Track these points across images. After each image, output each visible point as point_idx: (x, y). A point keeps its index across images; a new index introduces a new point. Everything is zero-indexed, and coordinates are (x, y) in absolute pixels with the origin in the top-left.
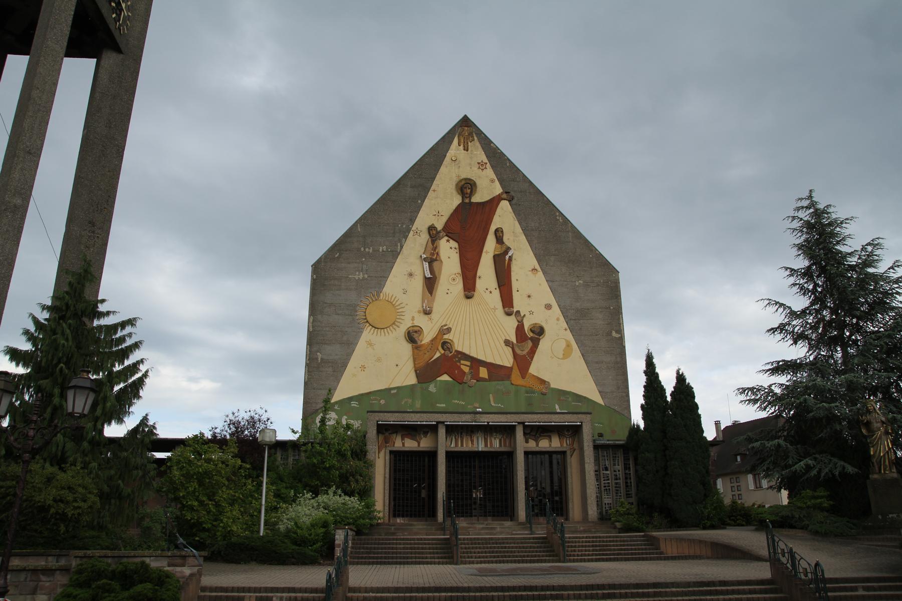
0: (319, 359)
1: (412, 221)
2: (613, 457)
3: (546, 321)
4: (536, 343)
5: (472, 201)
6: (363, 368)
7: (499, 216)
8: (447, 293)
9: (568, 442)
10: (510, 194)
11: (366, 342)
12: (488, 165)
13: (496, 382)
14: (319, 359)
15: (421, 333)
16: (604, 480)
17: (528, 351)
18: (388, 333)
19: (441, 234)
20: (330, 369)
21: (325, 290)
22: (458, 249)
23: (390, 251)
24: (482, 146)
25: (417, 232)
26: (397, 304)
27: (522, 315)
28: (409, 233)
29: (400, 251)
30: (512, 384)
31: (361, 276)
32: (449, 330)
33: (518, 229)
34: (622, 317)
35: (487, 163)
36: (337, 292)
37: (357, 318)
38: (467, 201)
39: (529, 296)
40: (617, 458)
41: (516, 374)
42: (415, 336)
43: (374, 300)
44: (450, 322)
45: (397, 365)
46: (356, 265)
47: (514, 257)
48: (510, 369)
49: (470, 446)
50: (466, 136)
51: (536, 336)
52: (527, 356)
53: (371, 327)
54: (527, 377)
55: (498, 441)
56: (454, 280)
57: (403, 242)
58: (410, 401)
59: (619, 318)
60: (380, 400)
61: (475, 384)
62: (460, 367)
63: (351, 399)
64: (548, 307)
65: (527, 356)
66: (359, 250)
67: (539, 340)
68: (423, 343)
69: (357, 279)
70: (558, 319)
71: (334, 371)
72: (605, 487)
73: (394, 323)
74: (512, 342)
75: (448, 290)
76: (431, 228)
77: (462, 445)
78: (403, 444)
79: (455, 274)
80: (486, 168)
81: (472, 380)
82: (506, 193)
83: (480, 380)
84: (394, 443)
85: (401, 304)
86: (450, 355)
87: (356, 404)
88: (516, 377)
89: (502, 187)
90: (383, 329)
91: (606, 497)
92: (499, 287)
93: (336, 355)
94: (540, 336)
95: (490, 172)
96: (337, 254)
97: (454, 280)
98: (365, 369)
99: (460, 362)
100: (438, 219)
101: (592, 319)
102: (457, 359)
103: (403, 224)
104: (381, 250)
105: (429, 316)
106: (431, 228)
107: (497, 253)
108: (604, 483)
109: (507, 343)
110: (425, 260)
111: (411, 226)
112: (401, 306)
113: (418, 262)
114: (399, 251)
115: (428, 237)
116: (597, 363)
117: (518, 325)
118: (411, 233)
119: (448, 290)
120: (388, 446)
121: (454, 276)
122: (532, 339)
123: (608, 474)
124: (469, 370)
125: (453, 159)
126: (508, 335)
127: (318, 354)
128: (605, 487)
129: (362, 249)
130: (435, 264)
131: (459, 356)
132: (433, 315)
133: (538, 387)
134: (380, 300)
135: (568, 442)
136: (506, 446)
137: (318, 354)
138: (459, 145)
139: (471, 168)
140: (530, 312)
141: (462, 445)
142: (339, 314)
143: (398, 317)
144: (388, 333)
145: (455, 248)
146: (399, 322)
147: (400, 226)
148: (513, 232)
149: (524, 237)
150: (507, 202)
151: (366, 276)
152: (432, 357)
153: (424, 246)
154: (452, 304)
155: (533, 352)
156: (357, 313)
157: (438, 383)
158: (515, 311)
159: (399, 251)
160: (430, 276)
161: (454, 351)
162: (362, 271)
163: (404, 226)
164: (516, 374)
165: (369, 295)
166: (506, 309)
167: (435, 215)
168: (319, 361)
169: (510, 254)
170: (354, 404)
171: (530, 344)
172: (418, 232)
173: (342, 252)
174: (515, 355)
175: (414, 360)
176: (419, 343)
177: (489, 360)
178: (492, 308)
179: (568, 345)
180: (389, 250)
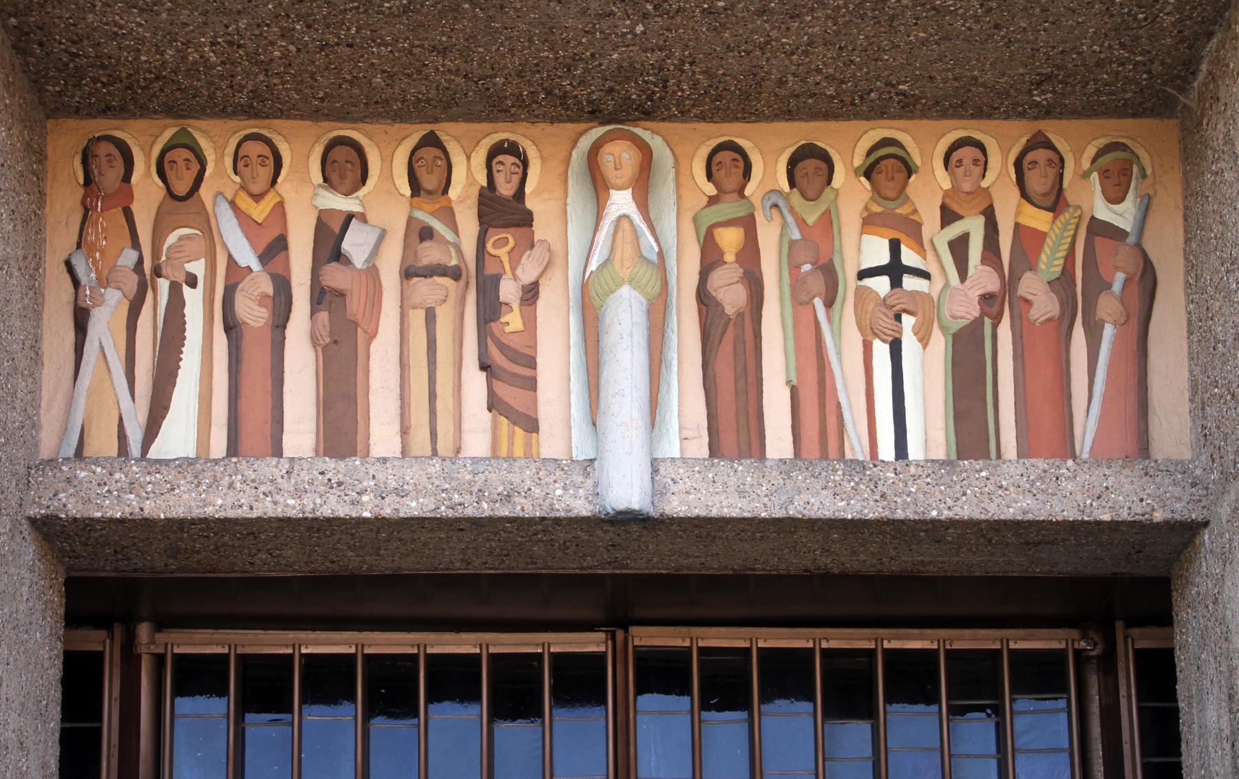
49: (477, 443)
136: (1066, 447)
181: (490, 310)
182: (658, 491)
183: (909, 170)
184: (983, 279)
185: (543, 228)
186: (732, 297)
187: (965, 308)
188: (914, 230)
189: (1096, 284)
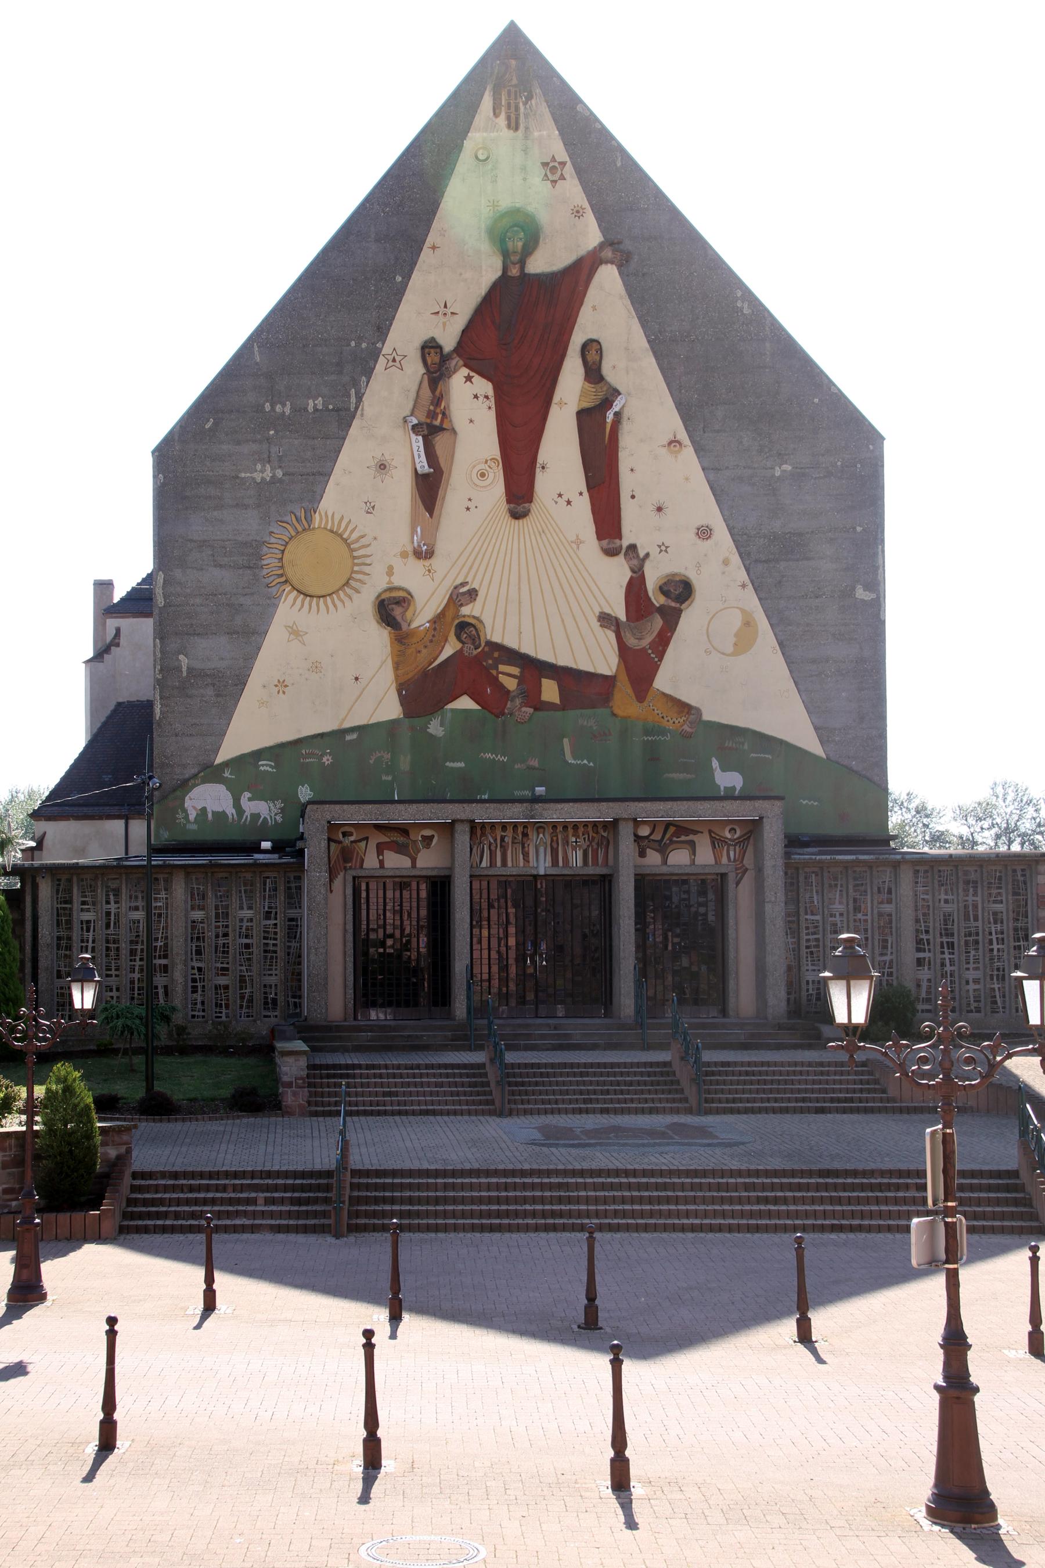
0: (184, 669)
1: (382, 331)
2: (830, 886)
3: (698, 566)
4: (671, 618)
5: (526, 271)
6: (282, 685)
7: (594, 308)
8: (468, 509)
9: (732, 854)
10: (621, 247)
11: (286, 626)
12: (569, 169)
13: (578, 712)
14: (184, 669)
15: (409, 605)
16: (808, 934)
17: (653, 641)
18: (335, 606)
19: (453, 363)
20: (210, 692)
21: (187, 508)
22: (493, 400)
23: (332, 410)
24: (553, 114)
25: (394, 360)
26: (354, 536)
27: (642, 554)
28: (376, 361)
29: (357, 408)
30: (614, 715)
31: (268, 474)
32: (473, 594)
33: (639, 340)
34: (883, 551)
35: (563, 164)
36: (215, 513)
37: (265, 572)
38: (514, 272)
39: (659, 509)
40: (839, 888)
41: (624, 690)
42: (397, 612)
43: (300, 529)
44: (475, 576)
45: (357, 679)
46: (255, 447)
47: (625, 415)
48: (609, 681)
49: (522, 864)
50: (515, 86)
51: (673, 604)
52: (650, 651)
53: (295, 592)
54: (649, 697)
55: (580, 853)
56: (483, 475)
57: (363, 384)
58: (387, 756)
59: (875, 554)
60: (322, 756)
61: (532, 715)
62: (497, 678)
63: (257, 755)
64: (704, 533)
65: (650, 651)
66: (259, 409)
67: (678, 613)
68: (414, 625)
69: (259, 480)
70: (726, 562)
71: (218, 696)
72: (807, 947)
73: (347, 584)
74: (617, 619)
75: (470, 500)
76: (429, 347)
77: (504, 863)
78: (381, 862)
79: (486, 462)
80: (562, 178)
81: (524, 709)
82: (612, 244)
83: (540, 706)
84: (362, 861)
85: (362, 537)
86: (475, 652)
87: (271, 766)
88: (624, 702)
89: (602, 232)
90: (323, 596)
91: (810, 968)
92: (589, 488)
93: (222, 659)
94: (682, 603)
95: (573, 190)
96: (208, 421)
97: (483, 475)
98: (286, 690)
99: (497, 669)
100: (444, 324)
101: (808, 559)
102: (490, 662)
103: (360, 339)
104: (310, 409)
105: (427, 563)
106: (429, 347)
107: (586, 405)
108: (808, 940)
109: (606, 620)
110: (415, 429)
111: (379, 345)
112: (363, 541)
113: (399, 434)
114: (353, 406)
115: (422, 370)
116: (814, 661)
117: (631, 578)
118: (382, 362)
119: (470, 500)
120: (351, 868)
121: (483, 466)
122: (662, 610)
123: (818, 921)
124: (518, 685)
125: (481, 157)
126: (607, 601)
127: (181, 657)
128: (807, 947)
129: (267, 407)
130: (440, 442)
131: (496, 655)
132: (435, 562)
133: (673, 722)
134: (314, 529)
135: (732, 854)
136: (598, 865)
137: (181, 657)
138: (496, 115)
139: (525, 179)
140: (659, 546)
141: (504, 863)
142: (221, 566)
143: (356, 568)
144: (335, 606)
145: (487, 397)
146: (360, 581)
147: (353, 344)
148: (627, 349)
149: (653, 360)
150: (614, 268)
151: (279, 473)
152: (435, 659)
153: (413, 395)
154: (480, 533)
155: (663, 641)
156: (265, 562)
157: (449, 715)
158: (625, 545)
159: (353, 406)
160: (426, 469)
161: (483, 644)
162: (269, 462)
163: (364, 345)
164: (624, 690)
165: (287, 518)
166: (605, 542)
167: (438, 313)
168: (185, 674)
169: (616, 407)
170: (265, 766)
171: (658, 622)
172: (398, 359)
173: (220, 415)
174: (623, 649)
175: (397, 666)
176: (404, 627)
177: (564, 660)
178: (570, 540)
179: (748, 623)
180: (331, 407)
181: (523, 847)
182: (545, 871)
183: (578, 828)
184: (588, 843)
185: (530, 837)
186: (555, 846)
187: (585, 847)
188: (578, 837)
189: (602, 843)
